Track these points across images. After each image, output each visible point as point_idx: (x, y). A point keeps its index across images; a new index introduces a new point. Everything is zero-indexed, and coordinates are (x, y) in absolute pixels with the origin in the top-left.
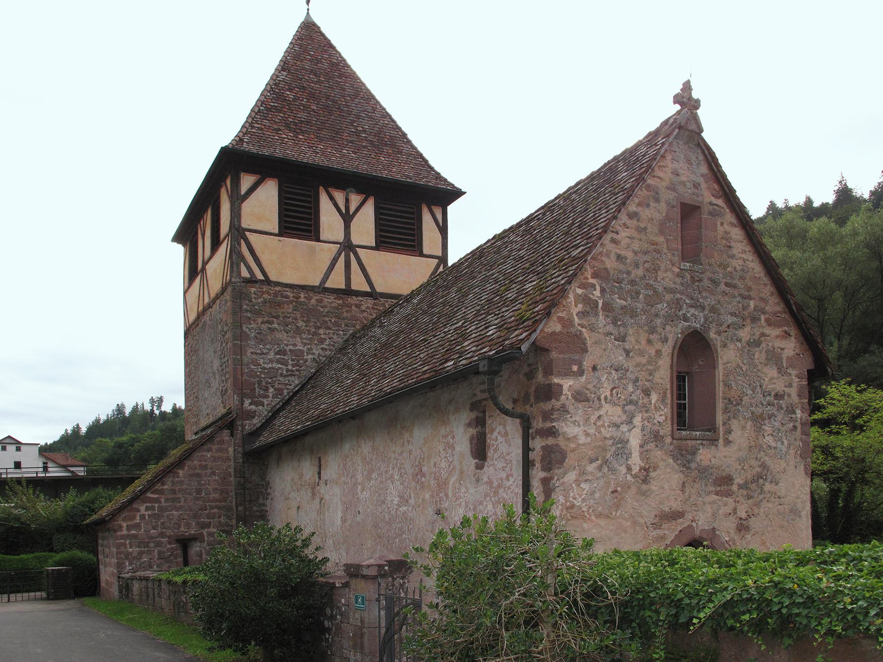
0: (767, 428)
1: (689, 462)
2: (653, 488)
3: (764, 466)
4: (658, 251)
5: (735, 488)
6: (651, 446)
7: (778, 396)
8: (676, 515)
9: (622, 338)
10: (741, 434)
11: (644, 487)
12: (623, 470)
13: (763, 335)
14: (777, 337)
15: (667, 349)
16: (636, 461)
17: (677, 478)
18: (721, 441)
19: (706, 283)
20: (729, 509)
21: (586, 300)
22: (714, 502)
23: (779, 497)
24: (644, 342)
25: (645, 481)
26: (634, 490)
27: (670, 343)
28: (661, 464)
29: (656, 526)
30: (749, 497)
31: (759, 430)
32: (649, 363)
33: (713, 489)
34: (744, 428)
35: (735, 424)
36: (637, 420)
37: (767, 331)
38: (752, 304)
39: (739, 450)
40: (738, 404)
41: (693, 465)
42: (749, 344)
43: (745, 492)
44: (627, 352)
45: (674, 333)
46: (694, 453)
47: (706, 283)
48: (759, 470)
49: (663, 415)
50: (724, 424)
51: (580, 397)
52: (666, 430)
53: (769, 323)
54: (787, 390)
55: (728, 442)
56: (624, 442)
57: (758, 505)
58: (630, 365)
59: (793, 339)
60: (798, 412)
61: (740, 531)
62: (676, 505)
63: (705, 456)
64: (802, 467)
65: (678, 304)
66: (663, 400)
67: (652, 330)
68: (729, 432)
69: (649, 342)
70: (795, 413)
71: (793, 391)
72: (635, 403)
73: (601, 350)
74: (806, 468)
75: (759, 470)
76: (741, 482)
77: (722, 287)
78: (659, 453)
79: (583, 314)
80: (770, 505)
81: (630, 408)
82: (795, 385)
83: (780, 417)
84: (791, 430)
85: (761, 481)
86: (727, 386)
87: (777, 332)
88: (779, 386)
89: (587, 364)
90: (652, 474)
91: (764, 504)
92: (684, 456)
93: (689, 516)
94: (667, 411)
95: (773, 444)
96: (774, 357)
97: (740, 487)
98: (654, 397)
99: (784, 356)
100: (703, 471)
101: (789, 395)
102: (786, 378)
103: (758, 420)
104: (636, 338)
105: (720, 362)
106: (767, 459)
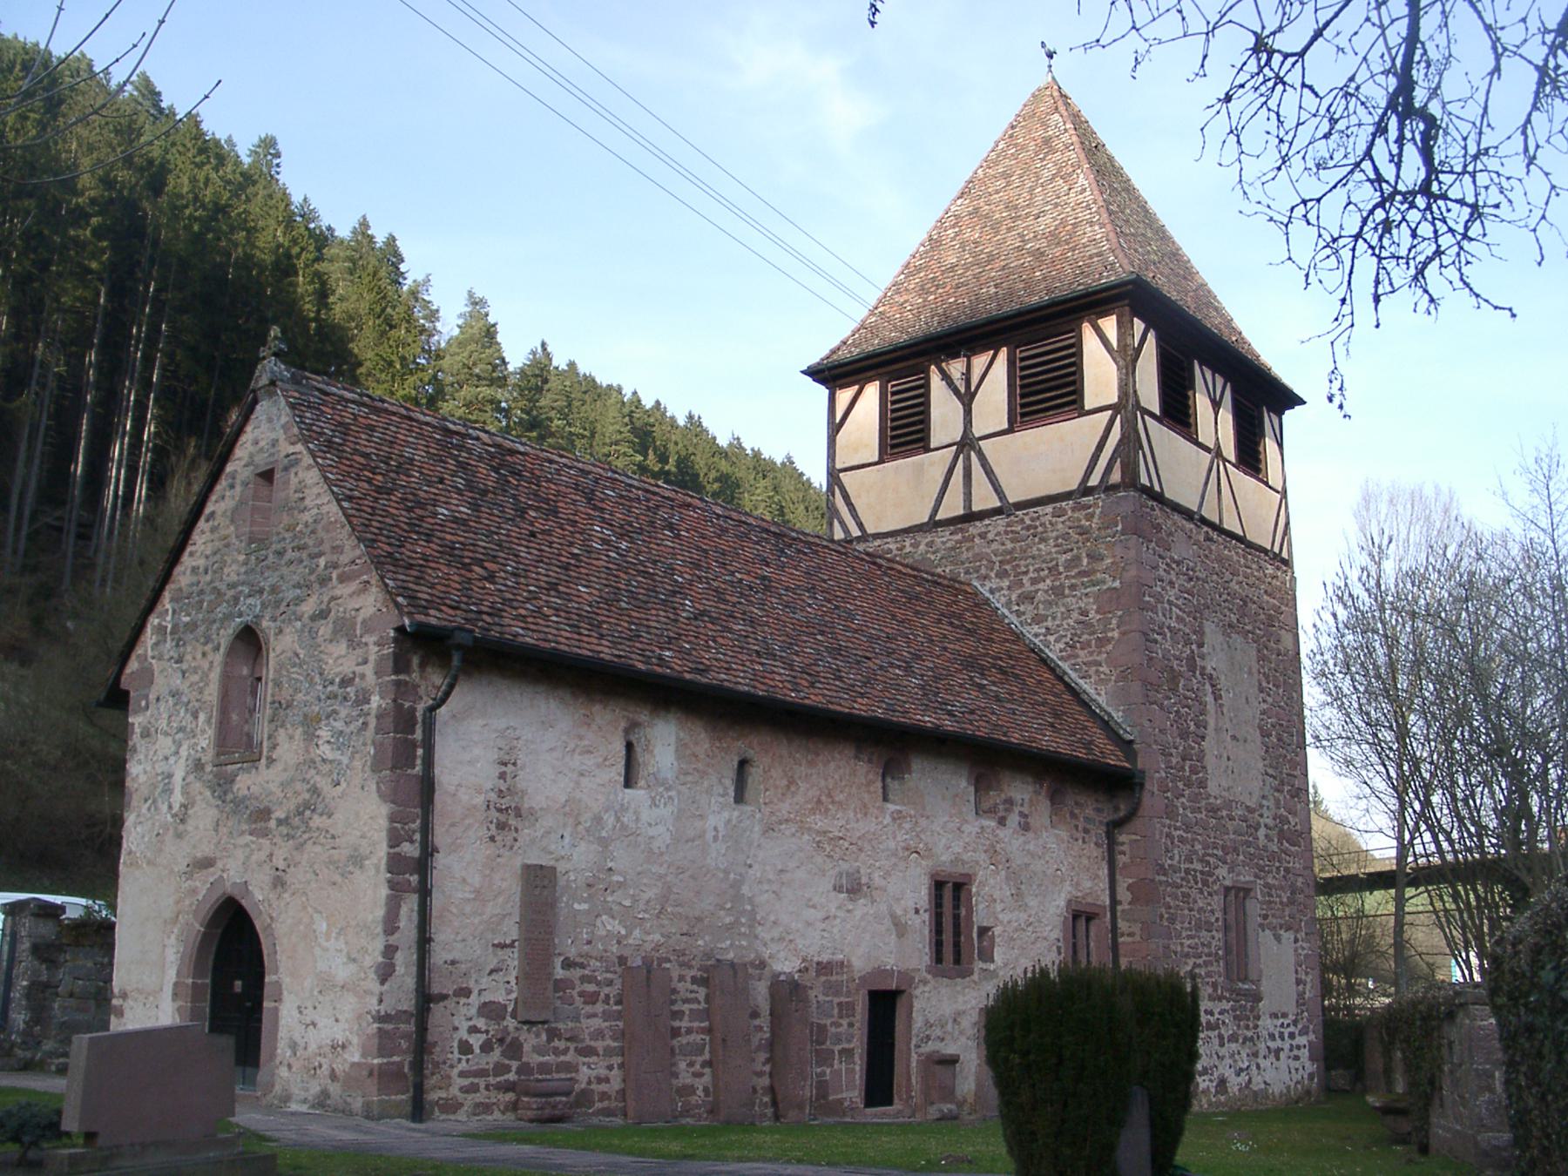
0: (324, 733)
1: (225, 793)
2: (190, 828)
3: (315, 791)
4: (227, 546)
5: (273, 824)
6: (191, 778)
7: (346, 682)
8: (207, 863)
9: (180, 661)
10: (289, 749)
11: (181, 827)
12: (165, 808)
13: (333, 598)
14: (351, 596)
15: (218, 658)
16: (177, 798)
17: (213, 813)
18: (263, 761)
19: (271, 558)
20: (263, 855)
21: (161, 630)
22: (247, 845)
23: (333, 837)
24: (199, 656)
25: (182, 821)
26: (171, 831)
27: (222, 650)
28: (199, 798)
29: (189, 875)
30: (289, 837)
31: (310, 737)
32: (201, 680)
33: (245, 827)
34: (291, 737)
35: (281, 735)
36: (184, 752)
37: (338, 592)
38: (322, 561)
39: (285, 770)
40: (288, 707)
41: (230, 797)
42: (313, 618)
43: (284, 830)
44: (184, 673)
45: (225, 636)
46: (233, 781)
47: (271, 558)
48: (307, 796)
49: (205, 740)
50: (269, 737)
51: (146, 734)
52: (208, 757)
53: (343, 579)
54: (359, 669)
55: (271, 761)
56: (170, 776)
57: (300, 847)
58: (184, 687)
59: (374, 589)
60: (375, 700)
61: (275, 887)
62: (206, 850)
63: (247, 783)
64: (374, 787)
65: (236, 599)
66: (208, 721)
67: (208, 640)
68: (274, 747)
69: (204, 654)
70: (368, 702)
71: (369, 670)
72: (181, 729)
73: (166, 678)
74: (378, 788)
75: (307, 796)
76: (283, 816)
77: (290, 555)
78: (198, 785)
79: (156, 644)
80: (318, 849)
81: (180, 735)
82: (372, 658)
83: (343, 712)
84: (360, 730)
85: (308, 813)
86: (278, 684)
87: (354, 586)
88: (348, 667)
89: (152, 697)
90: (190, 812)
91: (309, 845)
92: (222, 785)
93: (220, 865)
94: (210, 732)
95: (330, 755)
96: (346, 630)
97: (280, 822)
98: (202, 717)
99: (359, 620)
100: (238, 803)
101: (363, 676)
102: (359, 651)
103: (310, 724)
104: (193, 652)
105: (272, 655)
106: (318, 778)
